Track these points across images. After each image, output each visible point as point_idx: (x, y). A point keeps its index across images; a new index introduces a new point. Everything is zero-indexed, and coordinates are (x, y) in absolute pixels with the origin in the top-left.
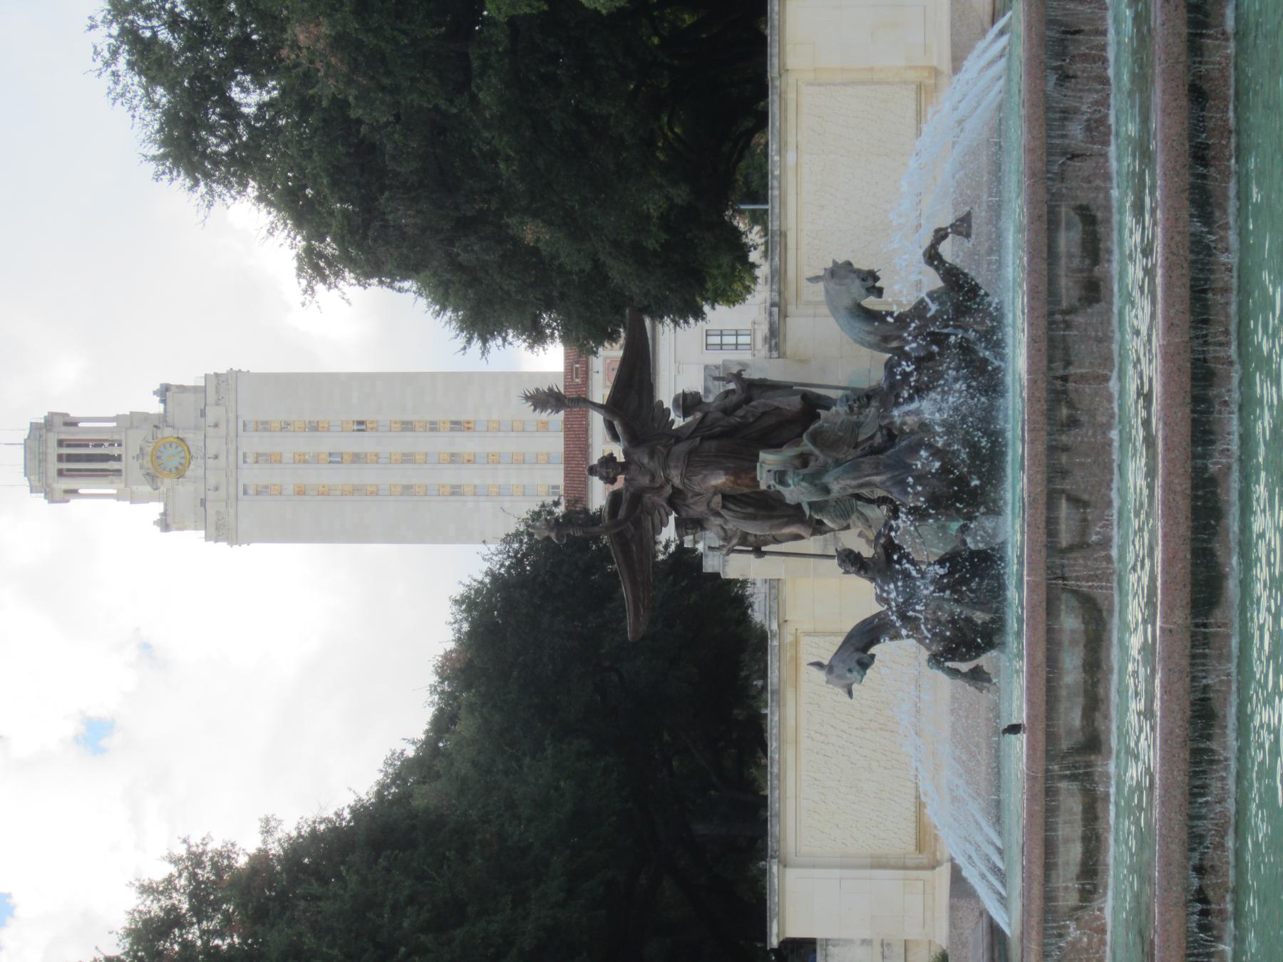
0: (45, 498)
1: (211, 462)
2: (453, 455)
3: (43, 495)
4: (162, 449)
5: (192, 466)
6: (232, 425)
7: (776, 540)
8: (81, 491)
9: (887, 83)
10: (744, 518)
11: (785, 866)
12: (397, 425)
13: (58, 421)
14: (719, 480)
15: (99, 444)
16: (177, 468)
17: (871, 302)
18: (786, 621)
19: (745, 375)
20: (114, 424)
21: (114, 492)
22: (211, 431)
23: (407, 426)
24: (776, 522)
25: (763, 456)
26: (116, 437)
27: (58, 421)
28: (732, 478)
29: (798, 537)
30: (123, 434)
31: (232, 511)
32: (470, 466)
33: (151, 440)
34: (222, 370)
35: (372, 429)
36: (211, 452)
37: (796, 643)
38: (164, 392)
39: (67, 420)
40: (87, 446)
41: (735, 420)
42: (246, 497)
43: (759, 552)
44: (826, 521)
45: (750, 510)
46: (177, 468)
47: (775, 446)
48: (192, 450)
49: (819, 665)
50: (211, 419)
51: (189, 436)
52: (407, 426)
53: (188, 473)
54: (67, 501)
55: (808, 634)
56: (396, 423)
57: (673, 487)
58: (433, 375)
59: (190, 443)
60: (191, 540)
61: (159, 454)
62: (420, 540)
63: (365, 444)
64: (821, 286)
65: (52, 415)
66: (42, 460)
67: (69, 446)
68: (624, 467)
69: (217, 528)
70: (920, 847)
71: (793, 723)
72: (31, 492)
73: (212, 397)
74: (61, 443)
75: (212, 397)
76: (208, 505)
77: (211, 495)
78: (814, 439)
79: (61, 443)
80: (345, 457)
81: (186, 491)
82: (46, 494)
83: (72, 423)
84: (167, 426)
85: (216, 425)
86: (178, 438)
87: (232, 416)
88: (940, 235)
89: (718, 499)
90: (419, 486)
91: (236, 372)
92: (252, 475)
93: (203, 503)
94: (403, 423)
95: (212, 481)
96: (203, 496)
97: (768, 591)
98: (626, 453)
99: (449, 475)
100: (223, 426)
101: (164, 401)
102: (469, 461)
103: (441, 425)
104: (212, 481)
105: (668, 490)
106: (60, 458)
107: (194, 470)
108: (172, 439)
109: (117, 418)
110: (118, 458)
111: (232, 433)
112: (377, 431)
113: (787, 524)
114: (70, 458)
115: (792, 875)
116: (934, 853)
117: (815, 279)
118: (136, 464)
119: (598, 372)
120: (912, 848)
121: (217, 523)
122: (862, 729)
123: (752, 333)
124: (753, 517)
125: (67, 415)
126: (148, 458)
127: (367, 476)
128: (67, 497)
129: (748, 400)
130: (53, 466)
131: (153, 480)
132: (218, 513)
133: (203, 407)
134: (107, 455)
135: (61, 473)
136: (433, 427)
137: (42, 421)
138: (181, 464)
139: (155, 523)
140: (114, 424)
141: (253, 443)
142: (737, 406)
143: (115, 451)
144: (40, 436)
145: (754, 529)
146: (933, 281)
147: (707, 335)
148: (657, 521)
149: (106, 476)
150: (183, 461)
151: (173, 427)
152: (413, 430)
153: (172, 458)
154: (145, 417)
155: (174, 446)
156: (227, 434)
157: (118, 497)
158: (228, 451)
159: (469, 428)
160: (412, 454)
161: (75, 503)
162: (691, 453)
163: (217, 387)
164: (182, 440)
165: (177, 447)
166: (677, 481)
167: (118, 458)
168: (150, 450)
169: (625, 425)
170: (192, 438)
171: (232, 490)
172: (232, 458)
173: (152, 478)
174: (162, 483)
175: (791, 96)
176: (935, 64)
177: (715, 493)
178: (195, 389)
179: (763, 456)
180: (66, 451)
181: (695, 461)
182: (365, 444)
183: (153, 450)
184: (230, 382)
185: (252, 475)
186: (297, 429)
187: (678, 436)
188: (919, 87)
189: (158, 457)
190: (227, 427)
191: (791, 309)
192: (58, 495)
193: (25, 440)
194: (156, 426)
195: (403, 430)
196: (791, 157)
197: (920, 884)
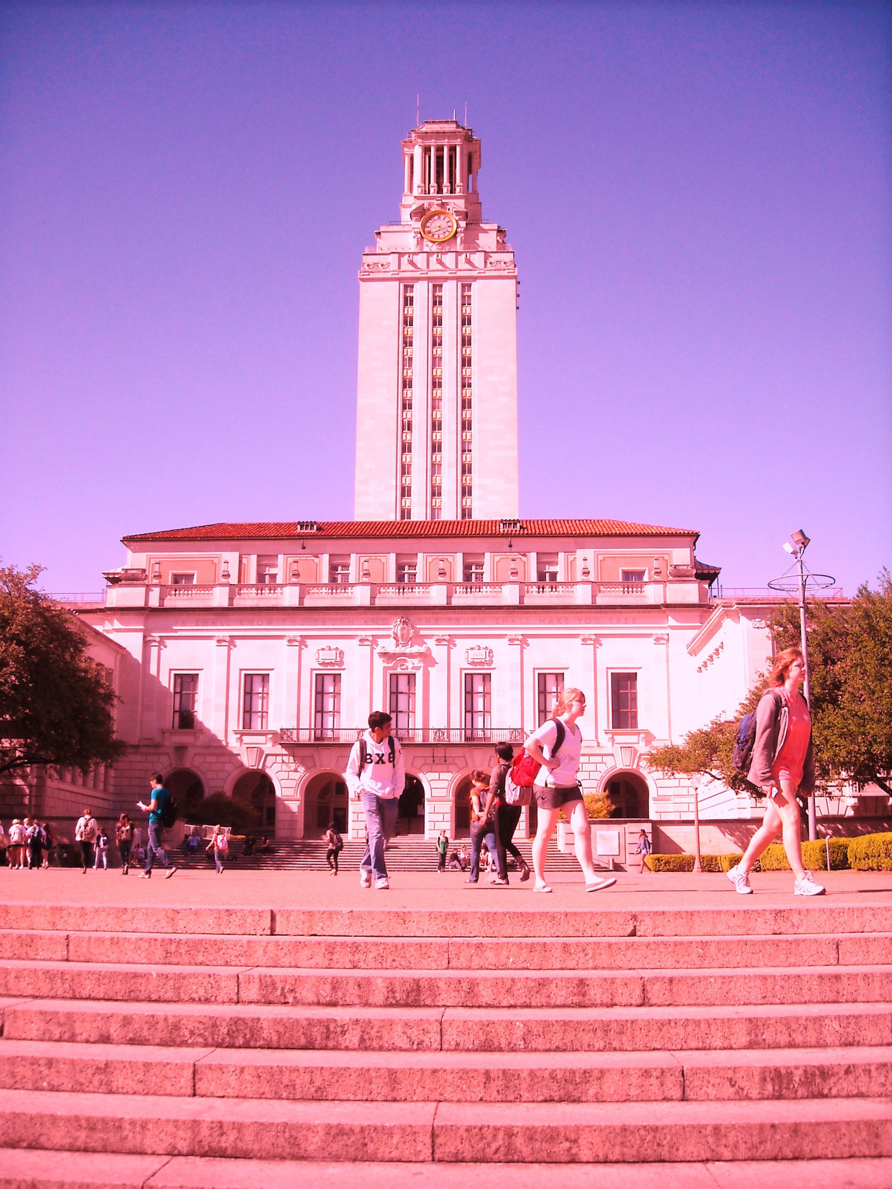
4: (447, 219)
5: (430, 244)
13: (472, 148)
31: (389, 275)
79: (453, 149)
81: (409, 242)
92: (421, 291)
110: (440, 191)
114: (440, 159)
135: (426, 150)
136: (465, 448)
138: (433, 235)
141: (449, 291)
149: (425, 184)
150: (436, 236)
155: (450, 229)
164: (455, 236)
167: (440, 191)
174: (417, 220)
180: (446, 150)
185: (421, 291)
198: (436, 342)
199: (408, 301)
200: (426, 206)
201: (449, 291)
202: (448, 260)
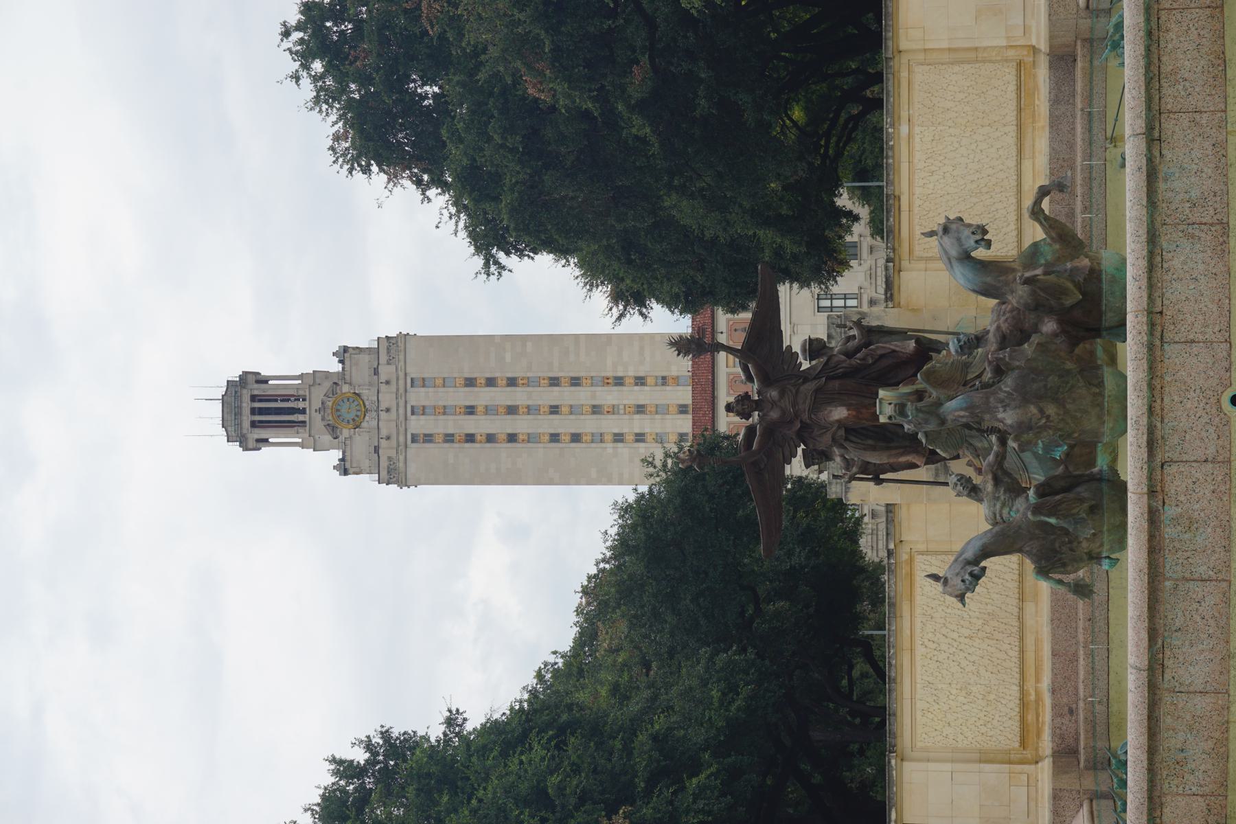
0: (240, 446)
1: (383, 415)
2: (594, 406)
3: (238, 443)
5: (367, 418)
6: (401, 382)
7: (894, 468)
8: (270, 440)
9: (991, 61)
10: (865, 449)
11: (902, 760)
12: (546, 381)
14: (839, 413)
15: (286, 398)
16: (354, 420)
17: (980, 253)
18: (901, 541)
19: (864, 323)
20: (300, 382)
21: (300, 440)
22: (383, 387)
23: (554, 382)
24: (894, 452)
25: (882, 393)
26: (301, 393)
27: (251, 379)
28: (854, 413)
29: (913, 466)
30: (307, 390)
31: (402, 458)
32: (610, 417)
33: (331, 396)
34: (393, 334)
35: (523, 384)
36: (383, 407)
37: (911, 560)
38: (344, 353)
39: (259, 378)
40: (276, 400)
41: (855, 361)
42: (414, 445)
43: (878, 481)
44: (938, 451)
45: (870, 442)
46: (354, 420)
47: (892, 384)
48: (367, 403)
49: (935, 577)
50: (383, 378)
51: (365, 392)
52: (554, 382)
53: (364, 424)
54: (259, 449)
55: (922, 553)
56: (544, 379)
57: (801, 422)
58: (577, 337)
59: (365, 398)
60: (366, 482)
61: (339, 407)
62: (566, 482)
63: (519, 396)
64: (934, 241)
65: (245, 373)
66: (238, 413)
67: (261, 401)
68: (758, 405)
69: (388, 472)
70: (1023, 743)
71: (908, 632)
72: (228, 441)
73: (383, 358)
74: (254, 398)
75: (383, 358)
76: (381, 451)
77: (383, 443)
78: (928, 377)
79: (254, 398)
80: (501, 410)
82: (241, 443)
83: (264, 381)
84: (345, 383)
85: (388, 383)
86: (355, 393)
87: (401, 374)
88: (1043, 192)
89: (842, 432)
90: (565, 435)
91: (405, 335)
92: (418, 425)
93: (377, 450)
94: (551, 379)
95: (384, 433)
96: (376, 444)
97: (875, 527)
98: (759, 393)
99: (588, 425)
100: (394, 382)
101: (341, 361)
102: (608, 412)
103: (584, 381)
104: (384, 433)
105: (798, 425)
106: (253, 411)
107: (369, 422)
108: (349, 395)
109: (301, 377)
110: (303, 411)
111: (402, 390)
112: (528, 386)
113: (902, 454)
114: (262, 411)
115: (907, 766)
116: (1037, 749)
117: (932, 234)
118: (318, 417)
119: (722, 333)
120: (1017, 745)
121: (388, 468)
122: (971, 638)
123: (858, 297)
124: (873, 448)
125: (259, 374)
126: (330, 411)
127: (521, 425)
128: (260, 445)
129: (867, 345)
130: (247, 418)
131: (333, 430)
132: (390, 458)
133: (376, 366)
134: (293, 408)
135: (254, 424)
137: (238, 379)
138: (357, 416)
139: (335, 467)
140: (300, 382)
141: (418, 397)
142: (858, 350)
143: (301, 405)
144: (236, 392)
145: (875, 458)
146: (1036, 233)
147: (818, 299)
148: (787, 453)
150: (359, 413)
151: (350, 384)
152: (557, 385)
153: (348, 411)
154: (327, 374)
155: (351, 400)
156: (398, 390)
157: (302, 446)
158: (398, 404)
159: (608, 383)
160: (557, 407)
161: (265, 450)
162: (817, 391)
163: (388, 349)
165: (354, 401)
166: (805, 417)
167: (303, 411)
168: (330, 404)
169: (757, 366)
170: (368, 395)
171: (402, 439)
172: (401, 411)
173: (333, 430)
175: (904, 74)
176: (1034, 42)
177: (839, 428)
178: (369, 350)
179: (882, 393)
181: (823, 398)
182: (519, 396)
183: (333, 404)
184: (399, 344)
186: (457, 385)
187: (806, 377)
188: (1019, 64)
189: (338, 410)
190: (397, 383)
191: (905, 264)
192: (251, 444)
193: (223, 396)
194: (335, 383)
195: (551, 385)
196: (904, 129)
197: (1025, 777)
198: (471, 410)
199: (428, 438)
200: (326, 423)
201: (418, 397)
202: (387, 399)
